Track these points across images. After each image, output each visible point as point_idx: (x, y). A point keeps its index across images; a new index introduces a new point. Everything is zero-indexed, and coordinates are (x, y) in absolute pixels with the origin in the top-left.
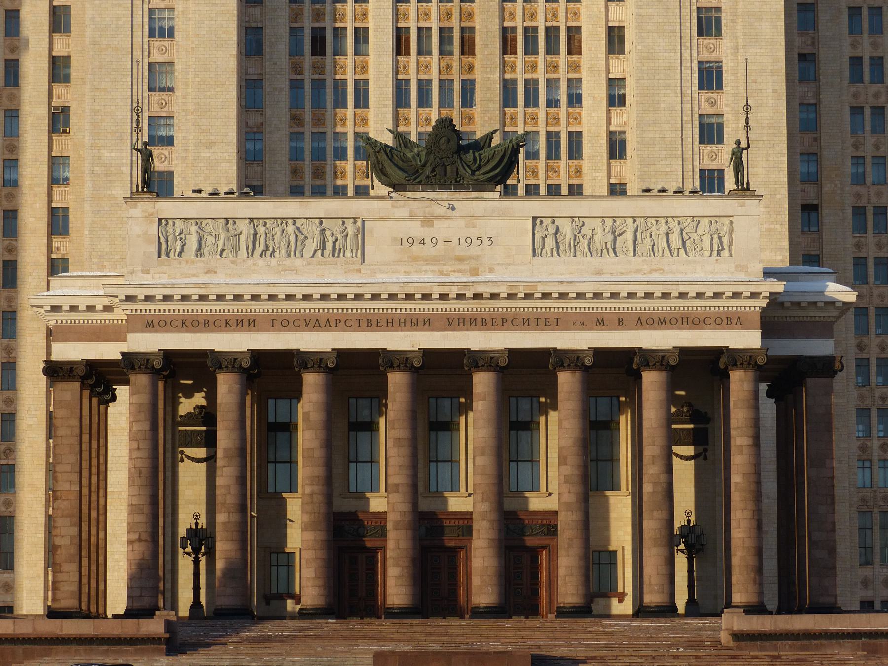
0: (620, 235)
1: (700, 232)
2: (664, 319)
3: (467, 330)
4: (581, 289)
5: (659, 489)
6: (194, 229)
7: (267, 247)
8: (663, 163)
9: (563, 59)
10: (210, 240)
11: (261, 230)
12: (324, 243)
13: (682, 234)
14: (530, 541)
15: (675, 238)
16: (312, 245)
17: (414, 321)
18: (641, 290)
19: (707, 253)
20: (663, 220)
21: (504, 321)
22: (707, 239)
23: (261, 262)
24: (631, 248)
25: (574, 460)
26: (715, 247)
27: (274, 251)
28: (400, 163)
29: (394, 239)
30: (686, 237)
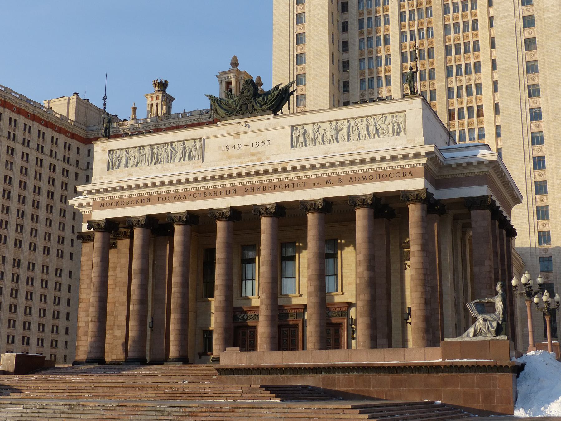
0: (340, 130)
1: (387, 123)
2: (365, 177)
3: (256, 194)
4: (313, 162)
5: (363, 281)
6: (125, 153)
7: (157, 159)
8: (515, 156)
9: (475, 119)
10: (132, 158)
11: (155, 151)
12: (185, 154)
13: (376, 125)
14: (335, 320)
15: (372, 129)
16: (179, 156)
17: (228, 191)
18: (347, 159)
19: (391, 135)
20: (364, 119)
21: (275, 187)
22: (391, 127)
23: (149, 168)
24: (346, 137)
25: (313, 266)
26: (396, 131)
27: (161, 161)
28: (225, 107)
29: (219, 147)
30: (378, 127)
